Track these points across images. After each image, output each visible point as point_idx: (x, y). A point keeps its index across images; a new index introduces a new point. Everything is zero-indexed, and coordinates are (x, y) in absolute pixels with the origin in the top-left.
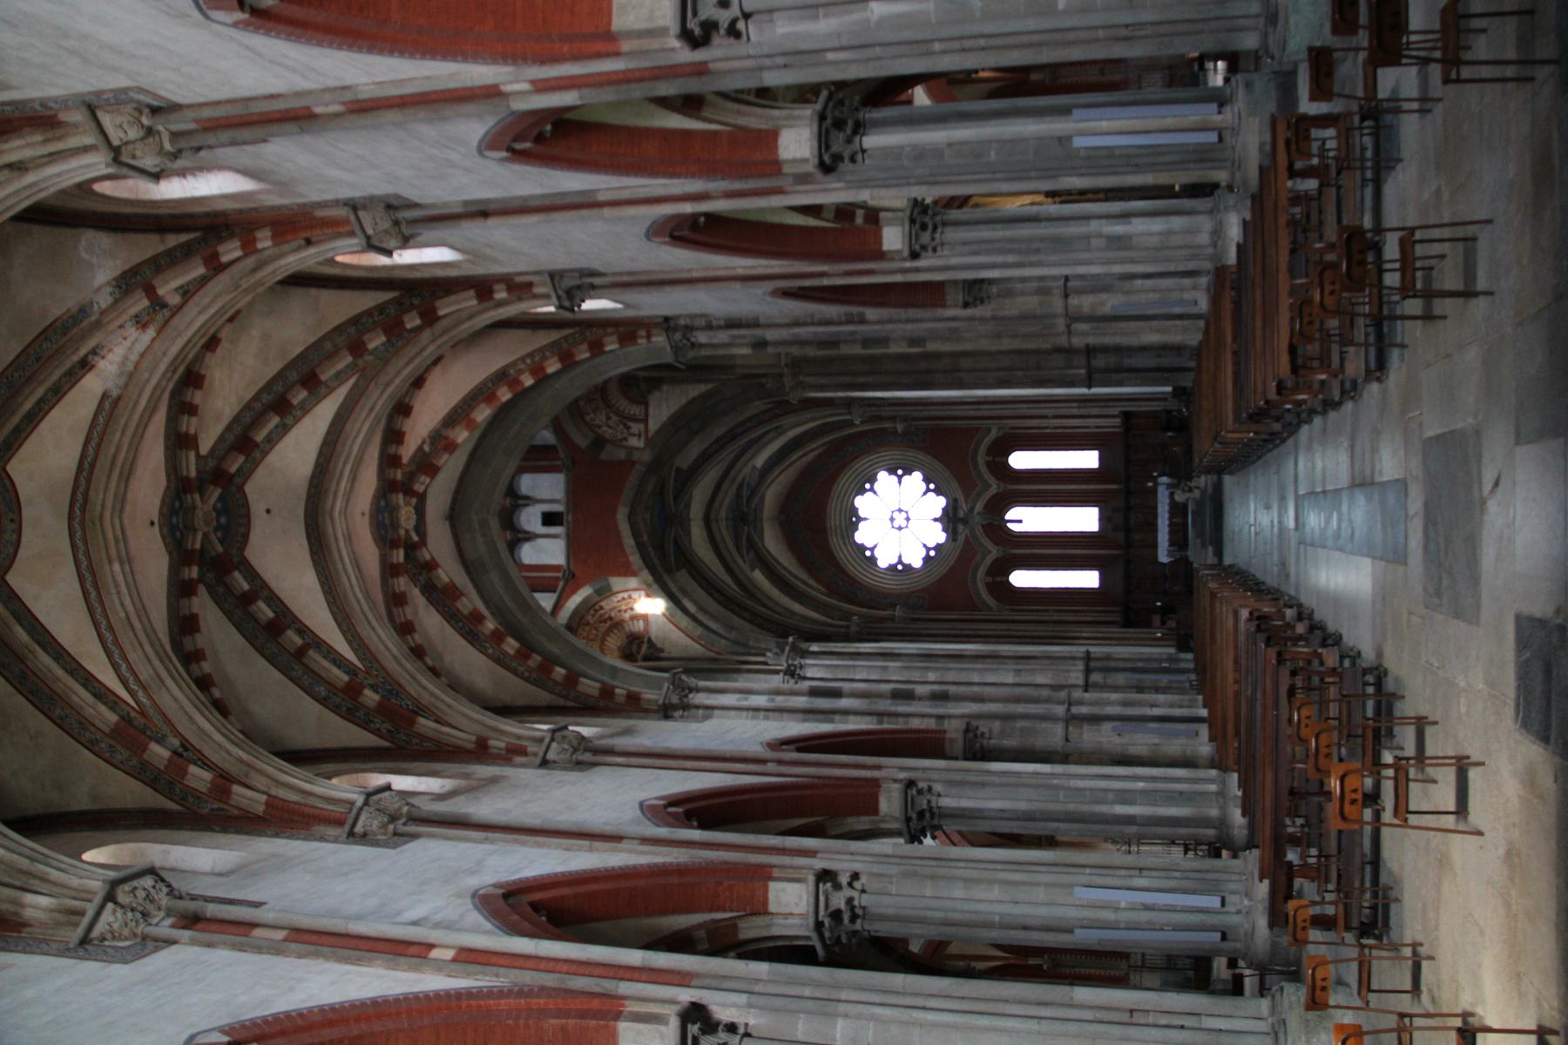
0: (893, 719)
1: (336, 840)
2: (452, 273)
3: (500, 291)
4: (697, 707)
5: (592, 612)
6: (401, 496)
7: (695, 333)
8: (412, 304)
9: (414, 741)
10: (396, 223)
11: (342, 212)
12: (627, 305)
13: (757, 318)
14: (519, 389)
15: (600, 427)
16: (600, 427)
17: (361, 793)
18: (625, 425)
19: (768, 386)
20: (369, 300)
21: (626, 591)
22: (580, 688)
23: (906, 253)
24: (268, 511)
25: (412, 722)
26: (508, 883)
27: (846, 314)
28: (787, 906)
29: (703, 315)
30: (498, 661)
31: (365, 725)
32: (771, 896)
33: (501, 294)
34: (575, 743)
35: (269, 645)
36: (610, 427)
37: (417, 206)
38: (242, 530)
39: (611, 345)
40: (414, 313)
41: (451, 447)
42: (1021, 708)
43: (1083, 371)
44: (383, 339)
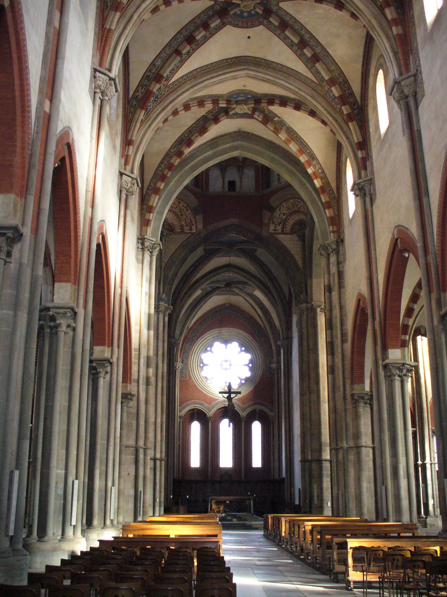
0: (137, 357)
1: (93, 63)
2: (372, 129)
3: (362, 153)
4: (143, 256)
5: (185, 205)
6: (253, 106)
7: (335, 255)
8: (354, 110)
9: (132, 109)
10: (407, 97)
11: (413, 71)
12: (351, 221)
13: (344, 287)
14: (306, 166)
15: (280, 210)
16: (280, 210)
17: (115, 76)
18: (280, 223)
19: (302, 296)
20: (356, 88)
21: (196, 223)
22: (153, 196)
23: (387, 361)
24: (249, 37)
25: (142, 109)
26: (74, 146)
27: (346, 333)
28: (58, 292)
29: (345, 260)
30: (167, 154)
31: (140, 84)
32: (63, 284)
33: (360, 154)
34: (131, 190)
35: (182, 37)
36: (279, 215)
37: (417, 107)
38: (240, 24)
39: (329, 213)
40: (350, 111)
41: (276, 131)
42: (142, 423)
43: (310, 458)
44: (337, 95)
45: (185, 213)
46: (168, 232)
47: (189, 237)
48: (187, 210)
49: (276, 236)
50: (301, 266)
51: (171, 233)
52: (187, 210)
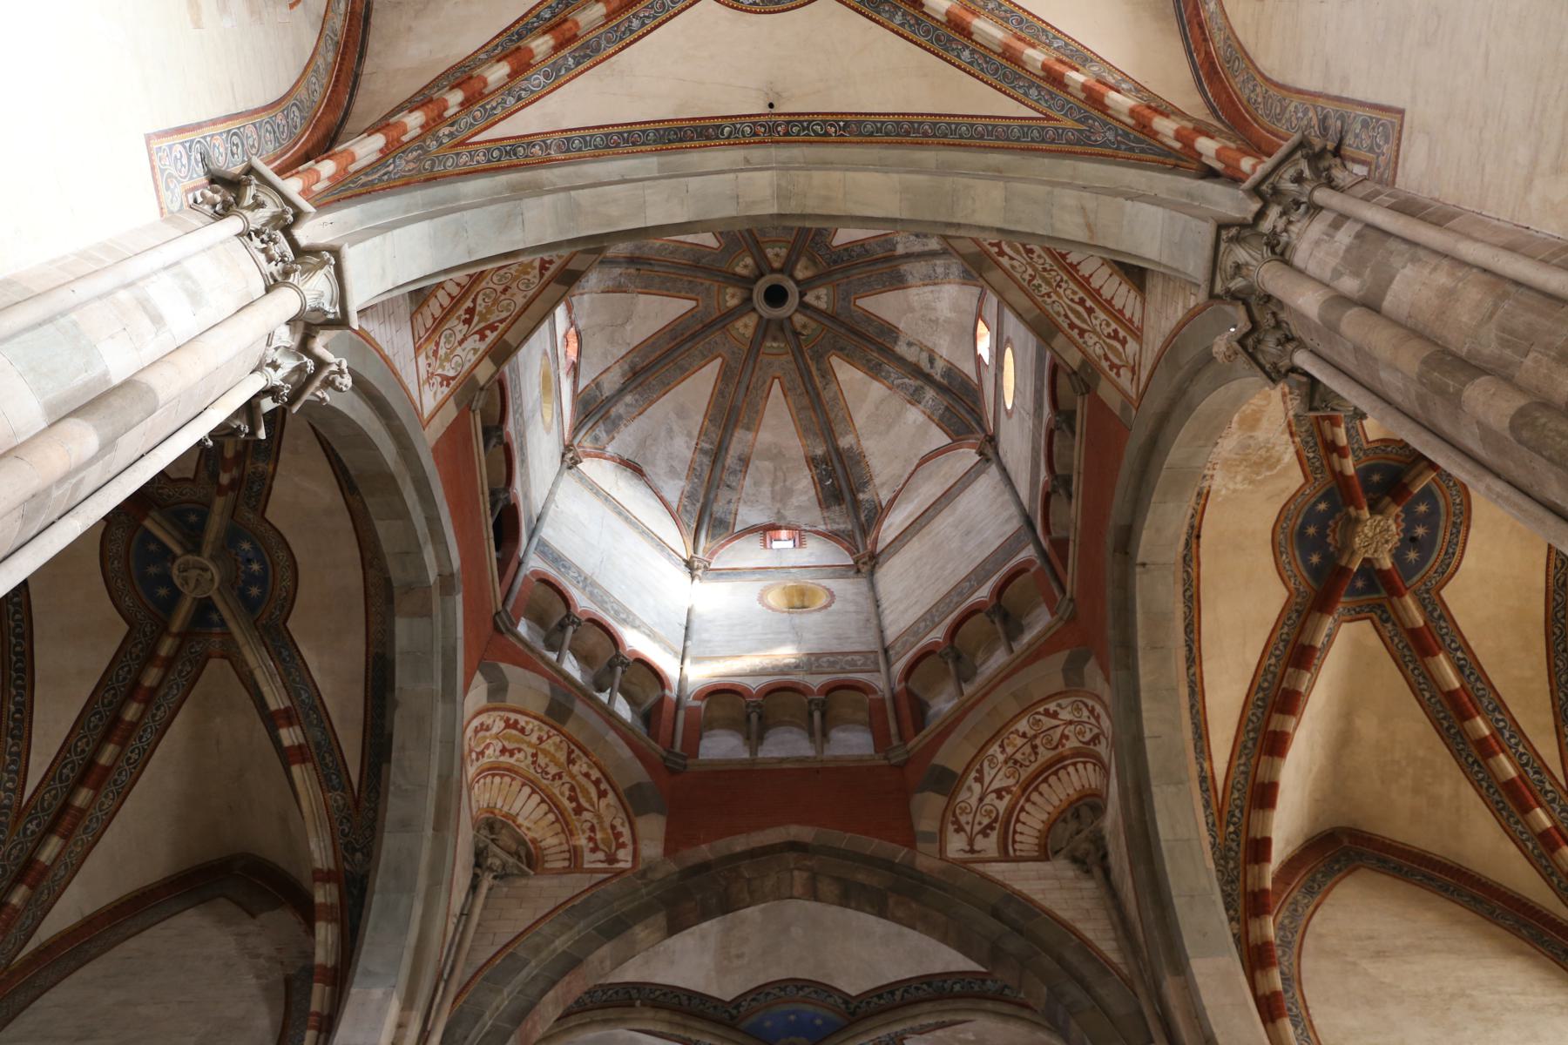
5: (595, 774)
15: (979, 780)
16: (979, 780)
18: (990, 827)
21: (635, 841)
36: (981, 800)
45: (593, 805)
46: (511, 860)
47: (604, 881)
48: (602, 794)
49: (979, 867)
50: (1115, 958)
51: (524, 867)
52: (602, 794)
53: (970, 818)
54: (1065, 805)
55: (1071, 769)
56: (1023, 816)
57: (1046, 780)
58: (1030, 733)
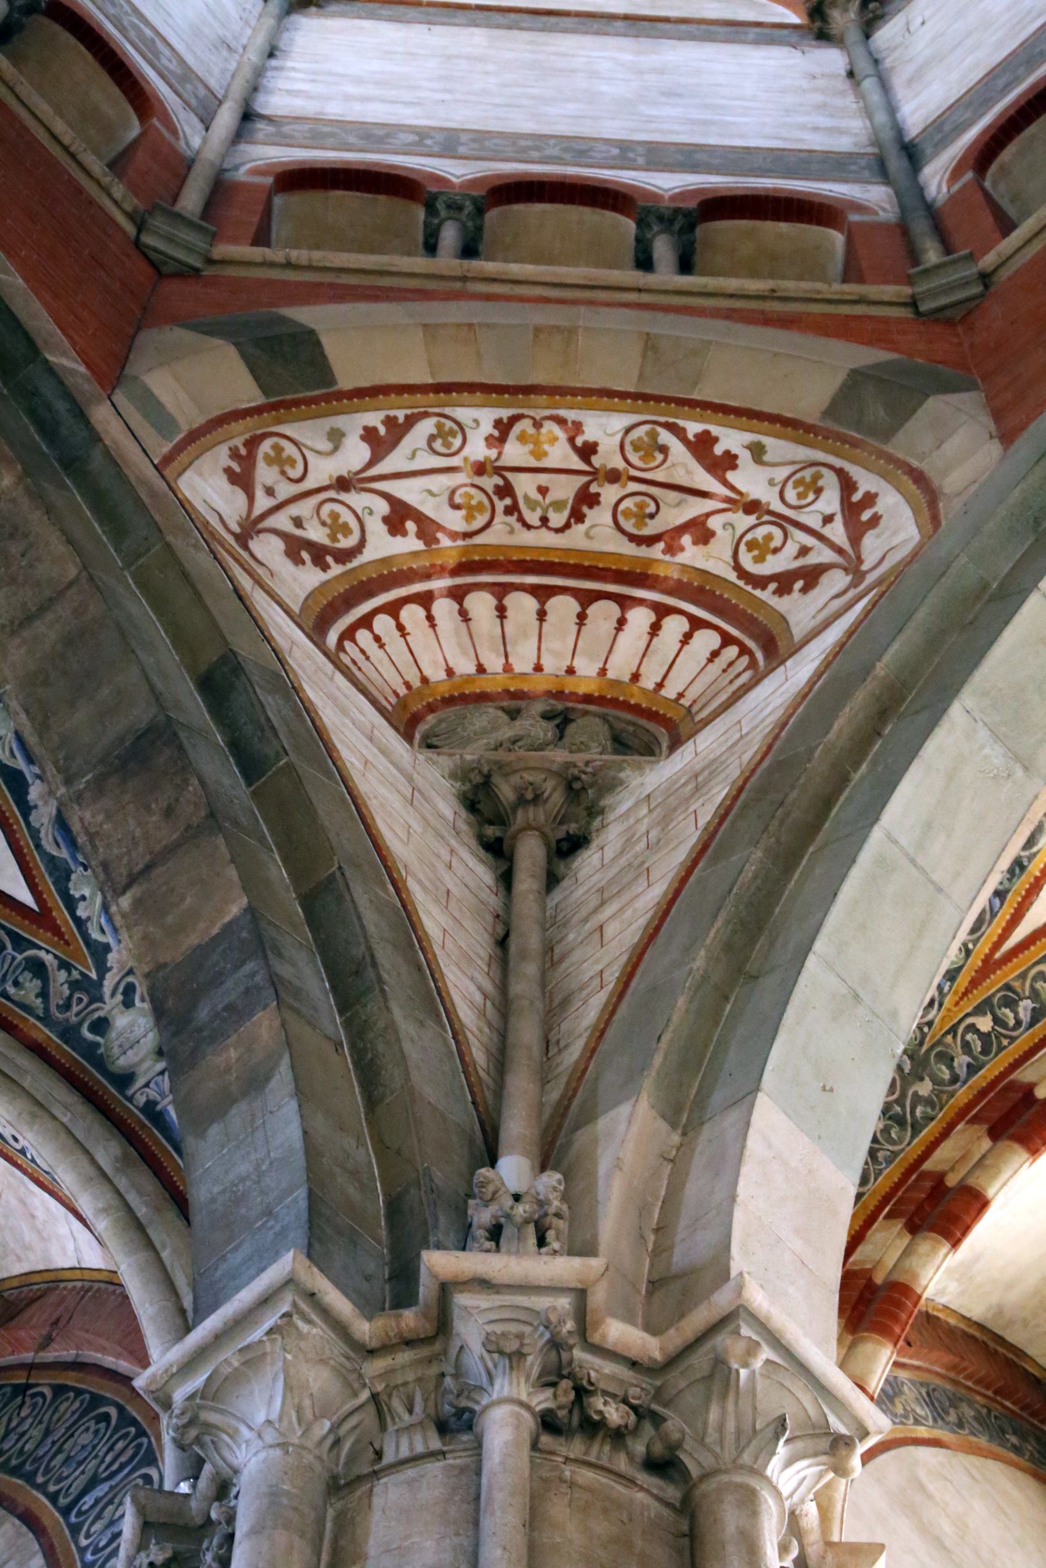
18: (319, 555)
36: (343, 484)
50: (466, 1014)
53: (283, 491)
54: (540, 684)
55: (640, 618)
56: (412, 614)
57: (543, 594)
58: (608, 457)
